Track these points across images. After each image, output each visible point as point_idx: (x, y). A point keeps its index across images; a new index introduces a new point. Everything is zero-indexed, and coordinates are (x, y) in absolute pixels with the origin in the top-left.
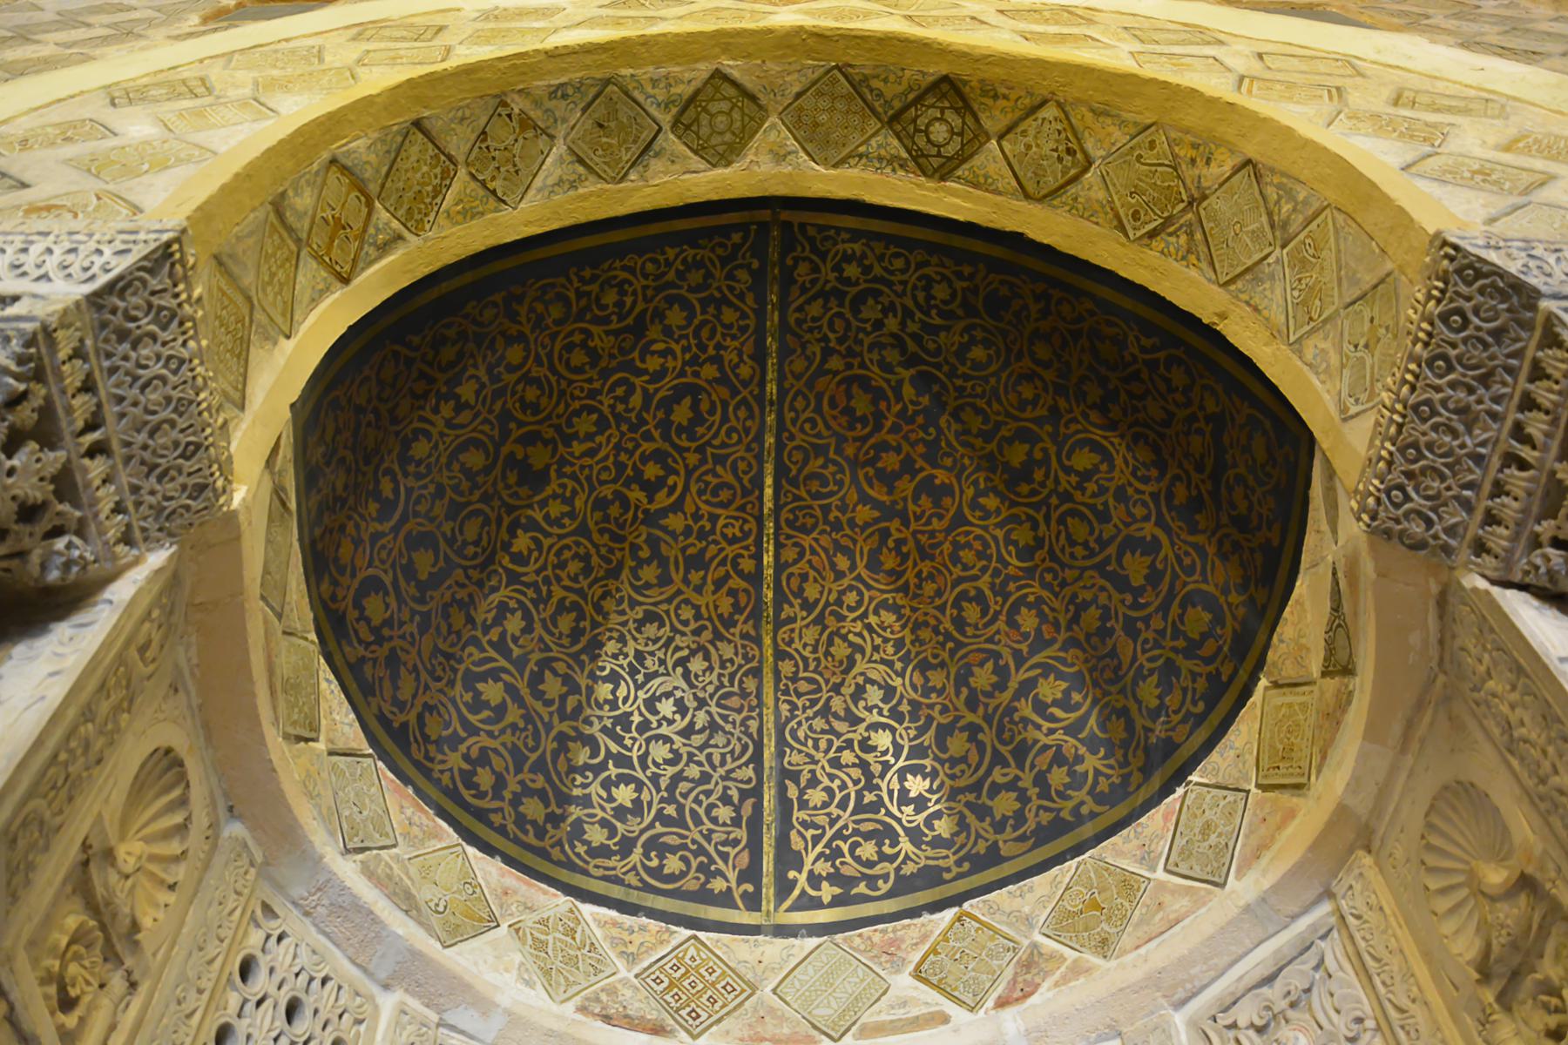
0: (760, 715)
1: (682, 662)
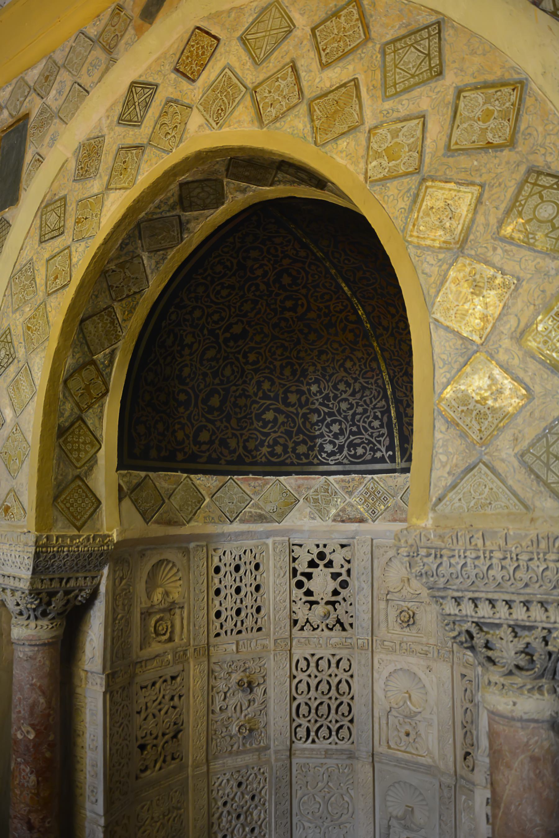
0: (382, 376)
1: (342, 365)
